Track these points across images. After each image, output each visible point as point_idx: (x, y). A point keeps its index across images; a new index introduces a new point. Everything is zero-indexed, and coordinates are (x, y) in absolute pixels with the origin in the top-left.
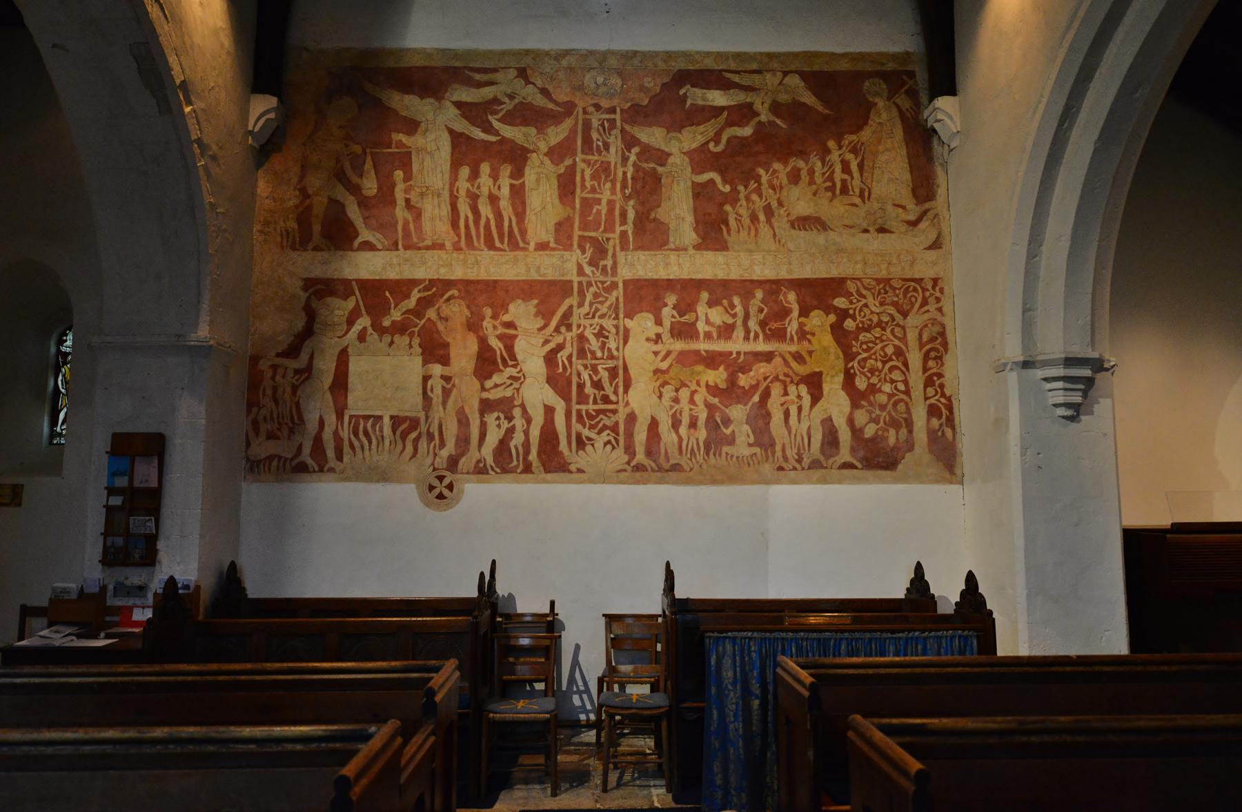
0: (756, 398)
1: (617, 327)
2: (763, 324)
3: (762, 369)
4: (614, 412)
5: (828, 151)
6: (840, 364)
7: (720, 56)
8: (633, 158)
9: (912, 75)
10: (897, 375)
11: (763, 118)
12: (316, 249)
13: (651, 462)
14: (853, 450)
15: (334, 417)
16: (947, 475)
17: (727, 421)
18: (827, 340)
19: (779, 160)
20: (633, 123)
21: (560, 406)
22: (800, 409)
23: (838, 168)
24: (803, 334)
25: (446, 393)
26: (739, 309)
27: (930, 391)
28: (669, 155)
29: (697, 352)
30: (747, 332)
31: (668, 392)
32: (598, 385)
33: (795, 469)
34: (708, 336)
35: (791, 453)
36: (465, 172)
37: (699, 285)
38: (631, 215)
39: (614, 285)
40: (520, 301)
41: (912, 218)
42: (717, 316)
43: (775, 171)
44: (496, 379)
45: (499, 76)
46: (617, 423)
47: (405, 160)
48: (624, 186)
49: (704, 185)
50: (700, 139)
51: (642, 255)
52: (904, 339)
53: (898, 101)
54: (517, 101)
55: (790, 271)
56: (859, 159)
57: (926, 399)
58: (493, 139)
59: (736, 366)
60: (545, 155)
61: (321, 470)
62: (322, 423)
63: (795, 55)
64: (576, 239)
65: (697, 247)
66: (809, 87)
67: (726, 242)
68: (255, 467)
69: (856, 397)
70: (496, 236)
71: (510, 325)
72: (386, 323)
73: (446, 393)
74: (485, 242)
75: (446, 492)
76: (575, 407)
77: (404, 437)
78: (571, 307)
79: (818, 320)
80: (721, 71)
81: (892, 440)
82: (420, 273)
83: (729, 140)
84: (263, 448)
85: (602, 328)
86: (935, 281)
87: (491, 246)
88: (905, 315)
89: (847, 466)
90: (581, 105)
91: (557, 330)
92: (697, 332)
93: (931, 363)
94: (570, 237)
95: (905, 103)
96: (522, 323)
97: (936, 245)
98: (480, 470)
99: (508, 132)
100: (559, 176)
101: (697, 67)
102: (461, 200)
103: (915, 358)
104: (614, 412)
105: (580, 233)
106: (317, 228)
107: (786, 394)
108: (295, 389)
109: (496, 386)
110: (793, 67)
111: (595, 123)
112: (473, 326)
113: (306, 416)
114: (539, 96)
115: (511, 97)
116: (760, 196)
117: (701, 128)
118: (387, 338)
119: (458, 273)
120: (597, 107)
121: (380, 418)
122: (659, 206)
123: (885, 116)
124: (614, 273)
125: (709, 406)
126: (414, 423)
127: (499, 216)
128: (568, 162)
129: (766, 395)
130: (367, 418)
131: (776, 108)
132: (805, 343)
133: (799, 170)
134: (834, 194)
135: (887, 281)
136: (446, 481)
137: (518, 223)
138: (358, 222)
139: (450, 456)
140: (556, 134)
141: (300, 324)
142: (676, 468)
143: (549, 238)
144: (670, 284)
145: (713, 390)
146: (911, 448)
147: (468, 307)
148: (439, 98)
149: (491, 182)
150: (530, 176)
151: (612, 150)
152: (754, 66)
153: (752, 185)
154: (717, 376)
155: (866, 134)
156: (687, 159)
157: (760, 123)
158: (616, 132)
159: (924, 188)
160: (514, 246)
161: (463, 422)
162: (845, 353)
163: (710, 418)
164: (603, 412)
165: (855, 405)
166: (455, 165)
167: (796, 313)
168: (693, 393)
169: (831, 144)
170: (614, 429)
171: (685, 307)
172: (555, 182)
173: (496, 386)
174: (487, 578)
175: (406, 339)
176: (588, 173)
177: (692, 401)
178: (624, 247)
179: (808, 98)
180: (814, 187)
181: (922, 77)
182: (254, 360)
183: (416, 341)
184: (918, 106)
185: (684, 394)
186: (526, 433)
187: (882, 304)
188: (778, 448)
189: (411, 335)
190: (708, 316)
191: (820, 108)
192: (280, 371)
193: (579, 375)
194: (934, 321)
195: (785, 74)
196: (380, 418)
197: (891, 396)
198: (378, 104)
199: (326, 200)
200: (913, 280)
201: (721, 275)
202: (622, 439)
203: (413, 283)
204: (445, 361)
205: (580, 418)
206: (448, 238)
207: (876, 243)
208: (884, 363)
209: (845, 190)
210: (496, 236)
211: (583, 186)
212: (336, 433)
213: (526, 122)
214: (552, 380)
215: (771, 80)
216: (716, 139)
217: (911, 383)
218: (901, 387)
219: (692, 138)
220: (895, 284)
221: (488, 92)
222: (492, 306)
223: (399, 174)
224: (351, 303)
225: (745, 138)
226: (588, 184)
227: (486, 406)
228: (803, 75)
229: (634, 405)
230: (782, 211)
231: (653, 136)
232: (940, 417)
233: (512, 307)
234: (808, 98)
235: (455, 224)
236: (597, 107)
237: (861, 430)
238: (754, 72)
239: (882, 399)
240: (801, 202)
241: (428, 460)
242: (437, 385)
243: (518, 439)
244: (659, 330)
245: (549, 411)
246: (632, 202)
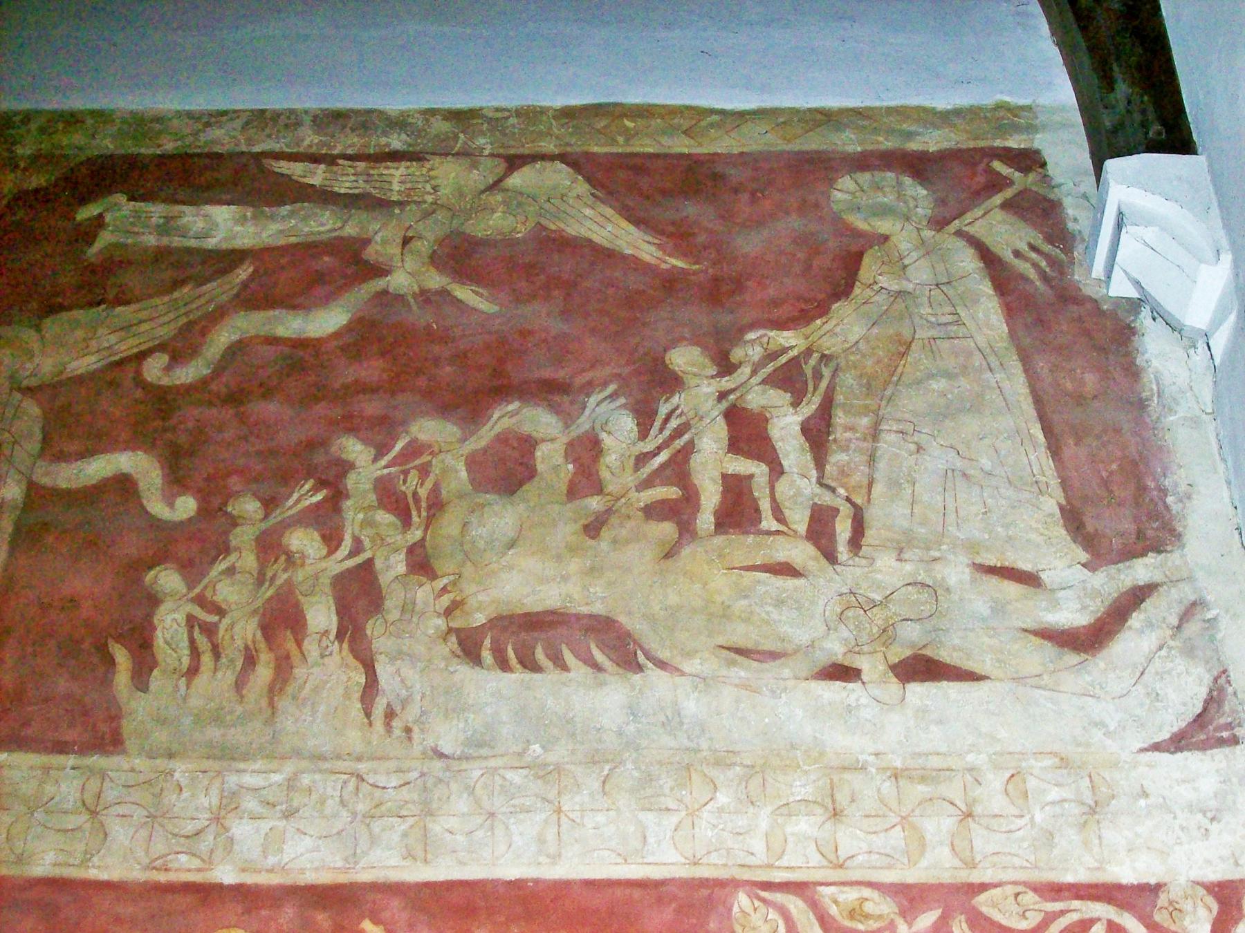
5: (671, 382)
9: (1029, 160)
11: (399, 281)
19: (444, 410)
41: (1072, 614)
53: (977, 230)
56: (810, 407)
67: (115, 716)
80: (258, 157)
83: (237, 349)
95: (1007, 234)
101: (169, 146)
110: (549, 146)
116: (332, 540)
123: (927, 269)
133: (528, 444)
134: (687, 530)
152: (396, 142)
153: (306, 496)
155: (845, 327)
180: (595, 503)
195: (514, 162)
207: (886, 722)
209: (738, 511)
230: (424, 593)
238: (395, 156)
240: (525, 570)
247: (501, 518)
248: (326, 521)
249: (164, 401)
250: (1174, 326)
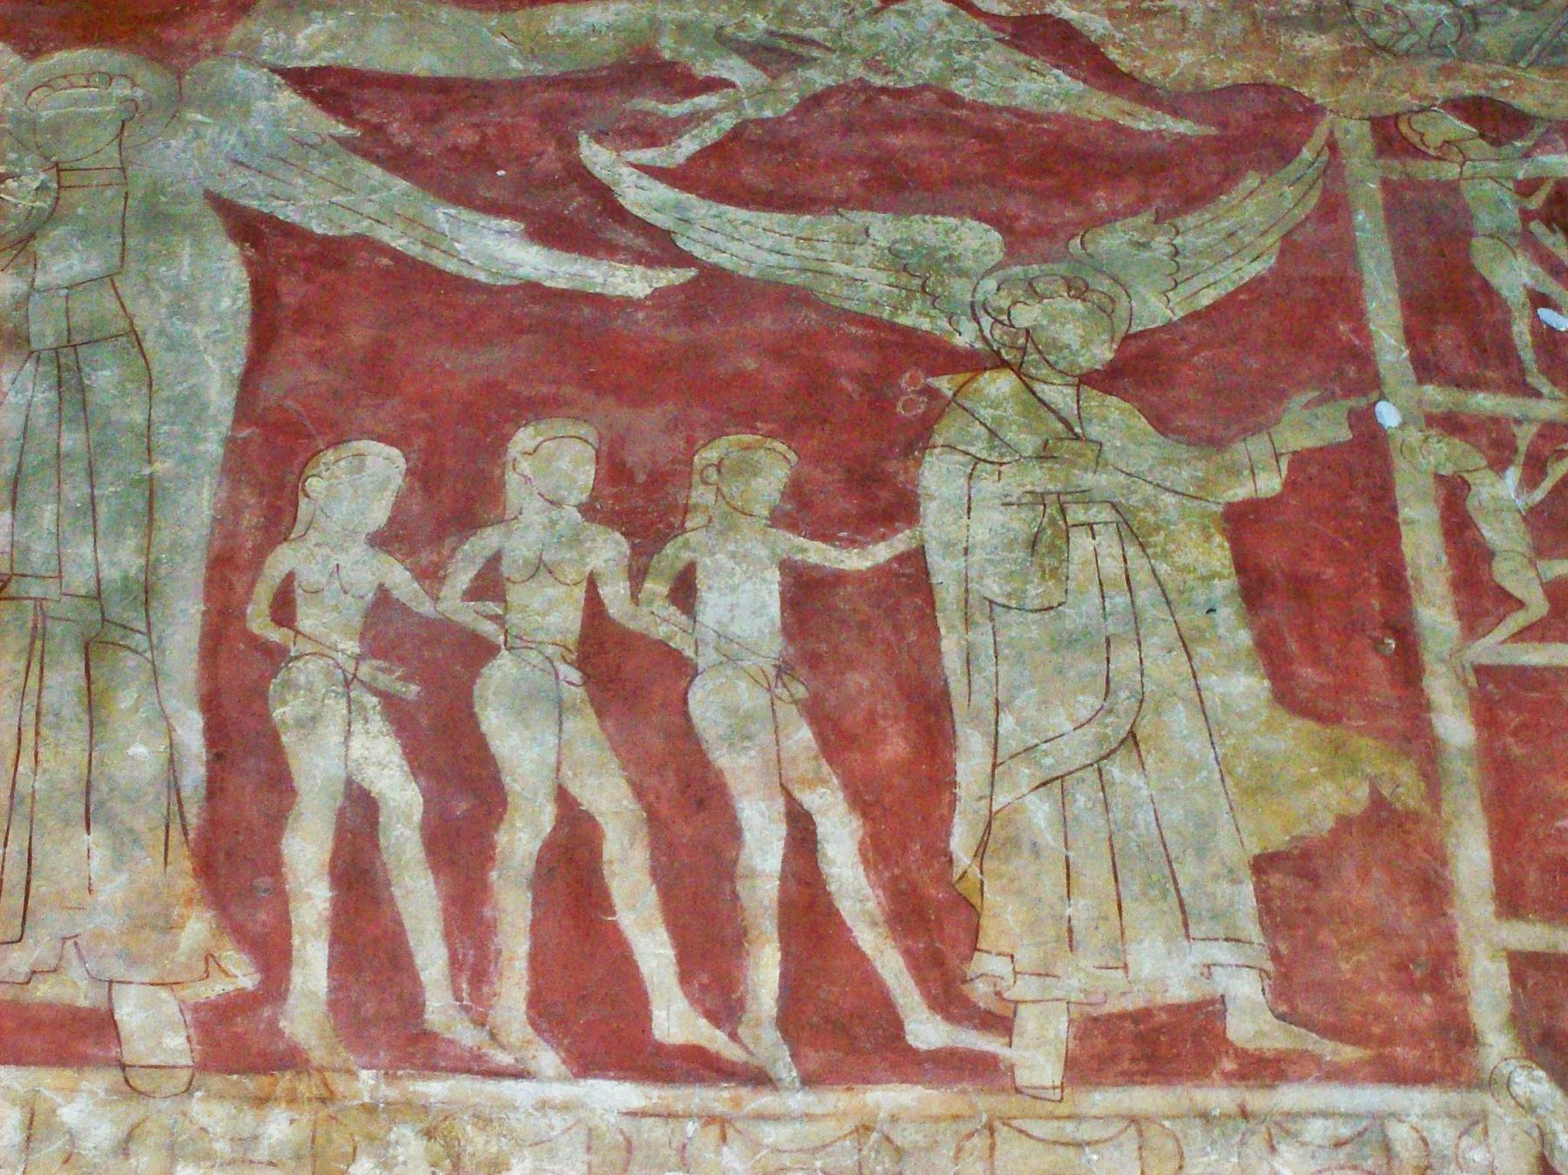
36: (361, 482)
54: (819, 79)
58: (628, 281)
60: (1106, 380)
70: (654, 952)
74: (545, 1012)
87: (597, 1024)
94: (1436, 971)
99: (745, 241)
100: (1242, 522)
102: (308, 671)
105: (1531, 935)
115: (774, 55)
120: (1495, 119)
128: (1310, 424)
137: (878, 852)
149: (607, 551)
150: (964, 511)
160: (841, 1030)
166: (272, 458)
176: (1501, 496)
210: (654, 952)
226: (1520, 574)
235: (230, 854)
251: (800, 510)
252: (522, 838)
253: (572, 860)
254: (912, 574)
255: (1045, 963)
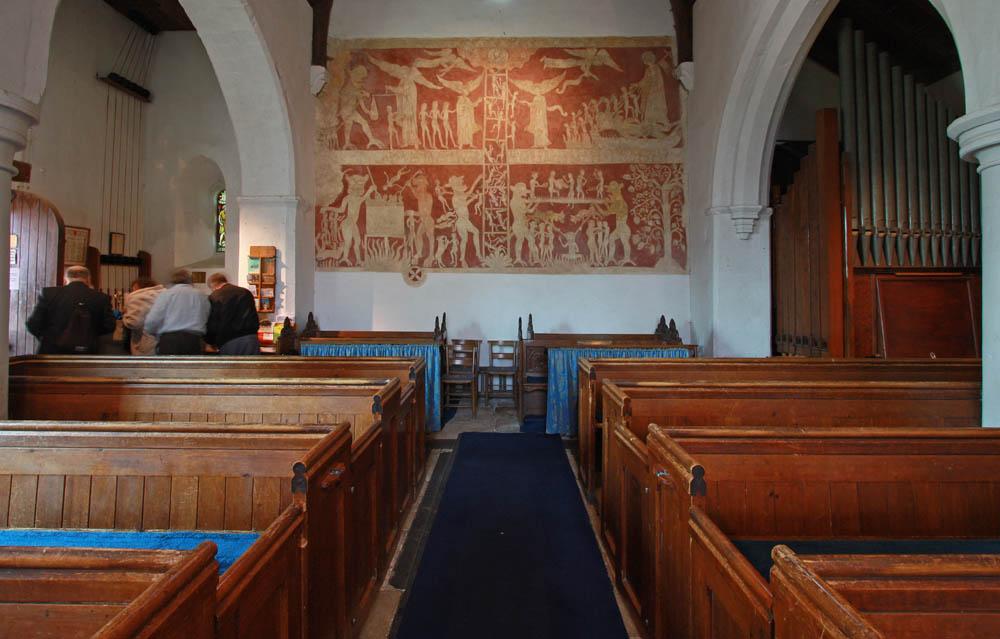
0: (580, 229)
1: (506, 190)
2: (584, 188)
3: (583, 213)
4: (505, 235)
6: (626, 211)
7: (562, 40)
8: (514, 98)
9: (669, 49)
10: (656, 217)
11: (586, 74)
12: (348, 149)
13: (524, 260)
14: (632, 257)
15: (359, 240)
16: (681, 269)
17: (565, 241)
18: (620, 198)
20: (515, 78)
21: (476, 232)
22: (604, 234)
23: (627, 103)
24: (606, 194)
25: (417, 225)
26: (571, 180)
27: (674, 225)
28: (534, 96)
29: (549, 204)
30: (576, 192)
31: (533, 225)
32: (496, 221)
33: (600, 266)
34: (555, 195)
35: (599, 258)
36: (424, 106)
37: (552, 167)
38: (514, 129)
39: (504, 168)
40: (454, 177)
41: (666, 130)
42: (560, 184)
43: (592, 105)
44: (443, 218)
45: (442, 53)
46: (506, 242)
47: (392, 100)
48: (510, 113)
49: (553, 113)
50: (551, 87)
51: (519, 151)
52: (660, 197)
54: (451, 67)
55: (599, 160)
57: (672, 229)
58: (439, 88)
59: (570, 210)
61: (354, 265)
62: (353, 241)
63: (605, 38)
64: (484, 143)
65: (549, 147)
66: (612, 56)
68: (320, 263)
69: (634, 228)
71: (449, 189)
72: (385, 188)
73: (417, 225)
75: (417, 277)
76: (484, 233)
77: (395, 248)
78: (482, 180)
79: (615, 187)
81: (652, 251)
82: (402, 162)
84: (324, 254)
85: (498, 191)
86: (679, 165)
88: (661, 184)
89: (628, 265)
90: (486, 68)
91: (474, 192)
92: (549, 194)
93: (675, 210)
95: (664, 64)
96: (454, 188)
97: (680, 145)
98: (435, 266)
99: (446, 84)
103: (666, 207)
104: (505, 235)
106: (347, 137)
107: (596, 226)
108: (339, 223)
109: (443, 221)
111: (494, 79)
112: (430, 190)
113: (345, 237)
114: (463, 64)
115: (449, 64)
117: (552, 81)
118: (386, 196)
119: (421, 161)
120: (495, 70)
121: (382, 239)
122: (528, 123)
123: (653, 73)
124: (505, 161)
125: (554, 232)
126: (400, 242)
127: (443, 129)
128: (480, 100)
129: (586, 227)
130: (376, 238)
131: (593, 69)
132: (607, 199)
135: (652, 165)
136: (418, 271)
138: (369, 135)
139: (419, 259)
140: (473, 85)
141: (340, 189)
142: (537, 265)
143: (469, 141)
144: (535, 167)
145: (557, 224)
146: (663, 256)
147: (428, 180)
148: (410, 66)
149: (438, 112)
150: (459, 108)
151: (504, 93)
153: (580, 112)
154: (560, 217)
155: (642, 83)
156: (544, 99)
157: (584, 77)
158: (506, 83)
159: (674, 113)
160: (451, 146)
161: (426, 240)
162: (628, 203)
163: (556, 239)
164: (499, 235)
165: (633, 232)
166: (419, 103)
167: (602, 183)
168: (547, 225)
169: (623, 89)
170: (505, 244)
171: (542, 179)
172: (472, 112)
173: (443, 221)
174: (441, 322)
175: (396, 197)
177: (546, 230)
178: (510, 147)
179: (611, 63)
181: (675, 51)
182: (318, 208)
183: (401, 198)
184: (672, 67)
185: (542, 226)
186: (459, 247)
187: (649, 178)
188: (592, 255)
189: (398, 195)
190: (554, 184)
191: (617, 68)
192: (332, 214)
193: (486, 215)
194: (677, 187)
195: (599, 49)
196: (382, 239)
197: (652, 227)
198: (377, 69)
199: (351, 123)
200: (666, 164)
201: (562, 162)
202: (509, 249)
203: (400, 167)
204: (416, 209)
205: (486, 238)
206: (416, 142)
207: (647, 144)
208: (650, 210)
211: (488, 114)
212: (361, 246)
213: (456, 79)
214: (472, 219)
215: (591, 53)
216: (560, 87)
217: (664, 221)
218: (658, 223)
219: (547, 86)
220: (657, 167)
221: (436, 62)
222: (439, 179)
223: (389, 108)
224: (366, 178)
225: (577, 87)
226: (491, 113)
227: (438, 232)
228: (608, 50)
229: (515, 232)
231: (526, 85)
232: (678, 238)
233: (450, 180)
234: (611, 63)
235: (420, 135)
236: (495, 70)
237: (637, 246)
239: (648, 229)
241: (410, 259)
242: (412, 222)
243: (454, 250)
244: (528, 192)
245: (470, 235)
246: (514, 123)
247: (603, 115)
248: (582, 115)
249: (560, 96)
250: (684, 88)
251: (449, 109)
252: (435, 133)
253: (437, 136)
254: (456, 113)
255: (462, 141)
